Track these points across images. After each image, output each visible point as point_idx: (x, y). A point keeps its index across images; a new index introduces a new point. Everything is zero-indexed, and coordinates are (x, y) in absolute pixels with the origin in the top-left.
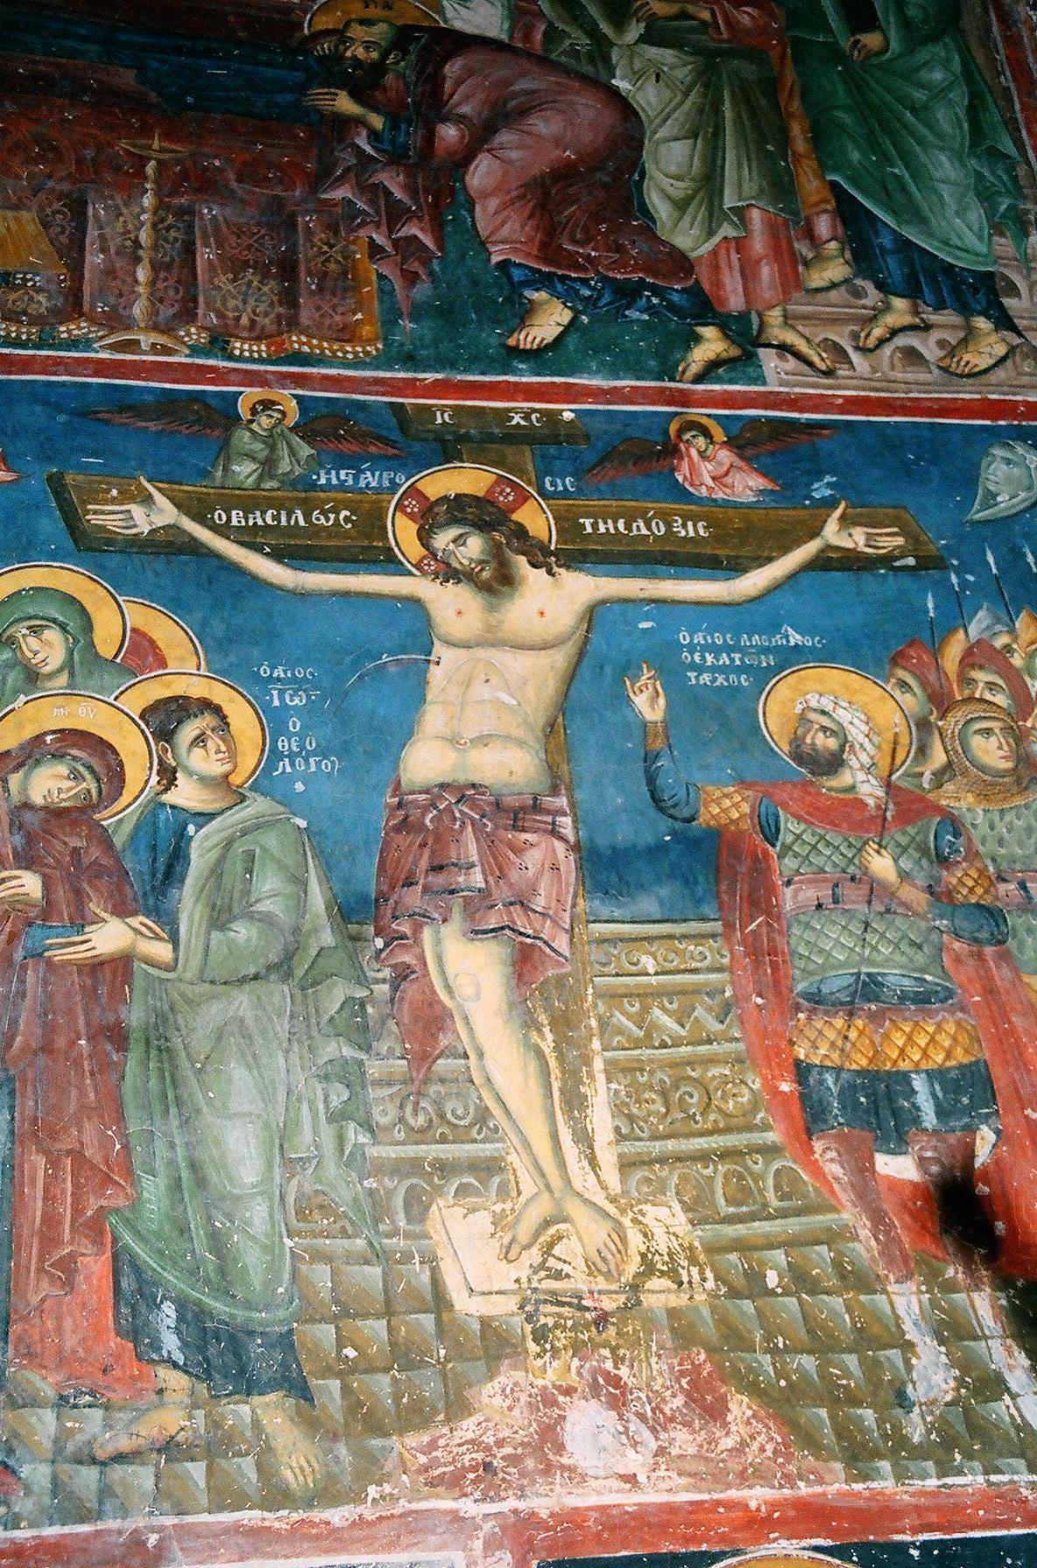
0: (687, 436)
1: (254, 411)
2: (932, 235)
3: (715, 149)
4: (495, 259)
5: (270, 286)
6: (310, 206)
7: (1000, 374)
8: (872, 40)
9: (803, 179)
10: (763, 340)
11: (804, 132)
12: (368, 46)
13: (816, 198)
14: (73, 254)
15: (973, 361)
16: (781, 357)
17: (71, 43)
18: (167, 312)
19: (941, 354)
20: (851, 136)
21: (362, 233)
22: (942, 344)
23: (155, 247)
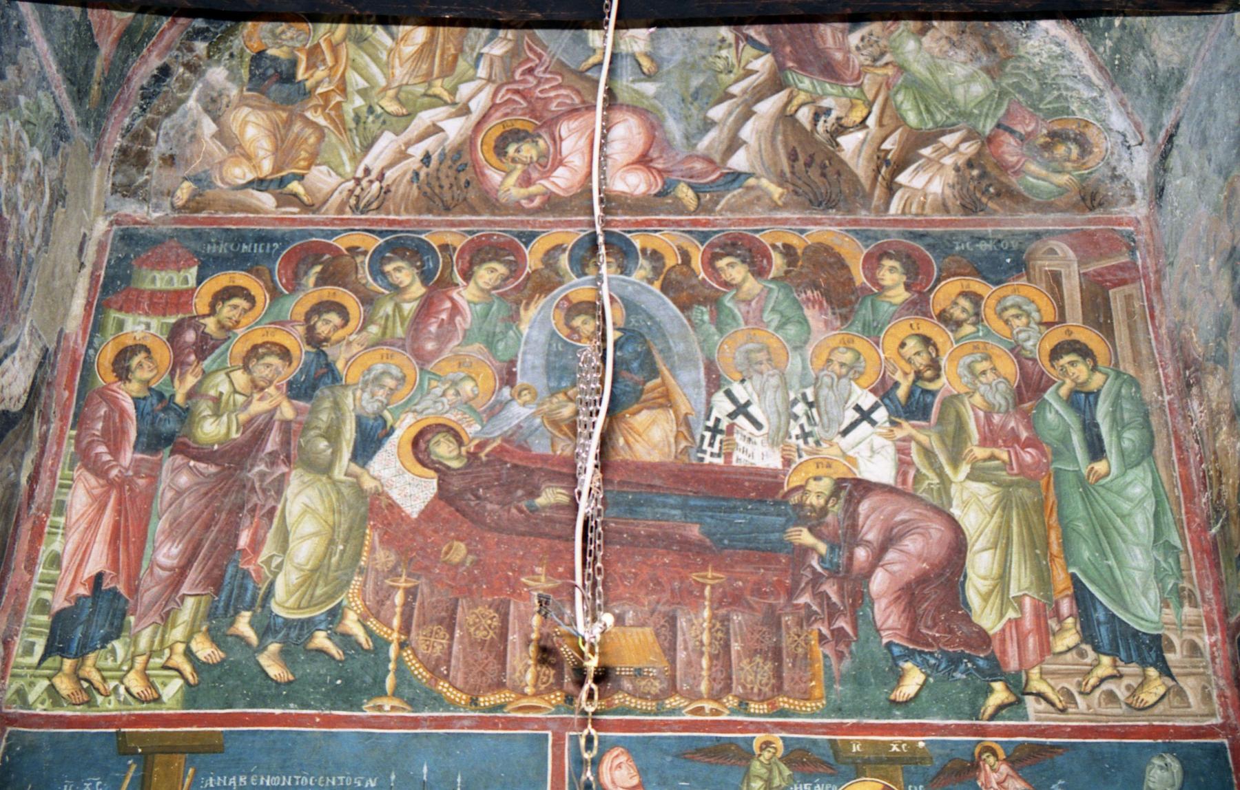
0: (984, 756)
1: (762, 749)
2: (1126, 609)
3: (1006, 555)
4: (885, 641)
5: (769, 665)
6: (788, 609)
7: (1160, 708)
8: (1100, 467)
9: (1055, 573)
10: (1028, 690)
11: (1058, 539)
12: (819, 495)
13: (1061, 587)
14: (670, 651)
15: (1146, 699)
16: (1038, 702)
17: (666, 510)
18: (718, 687)
19: (1127, 694)
20: (1086, 541)
21: (815, 627)
22: (1128, 687)
23: (711, 644)
